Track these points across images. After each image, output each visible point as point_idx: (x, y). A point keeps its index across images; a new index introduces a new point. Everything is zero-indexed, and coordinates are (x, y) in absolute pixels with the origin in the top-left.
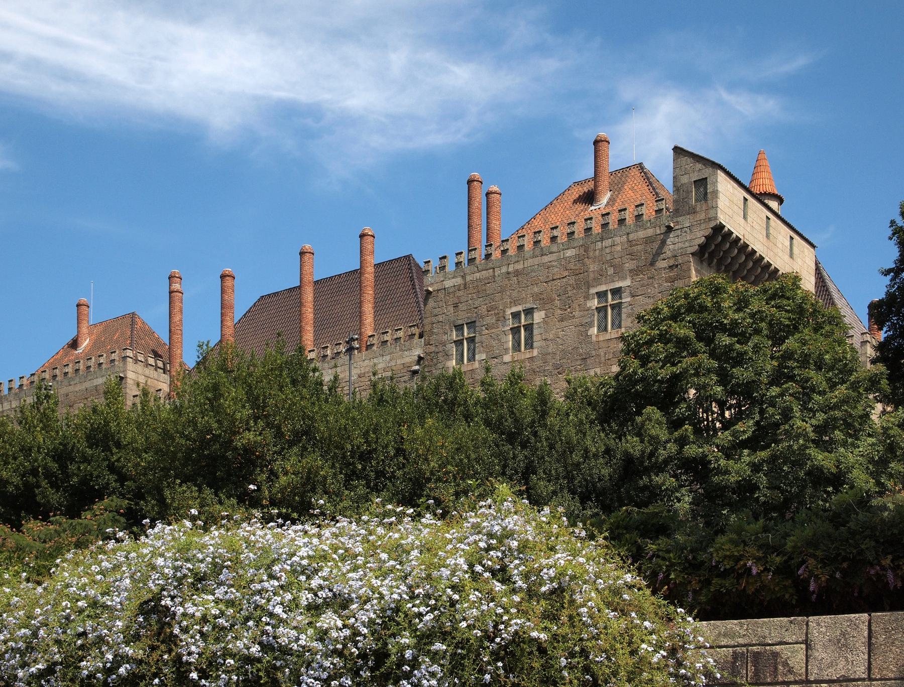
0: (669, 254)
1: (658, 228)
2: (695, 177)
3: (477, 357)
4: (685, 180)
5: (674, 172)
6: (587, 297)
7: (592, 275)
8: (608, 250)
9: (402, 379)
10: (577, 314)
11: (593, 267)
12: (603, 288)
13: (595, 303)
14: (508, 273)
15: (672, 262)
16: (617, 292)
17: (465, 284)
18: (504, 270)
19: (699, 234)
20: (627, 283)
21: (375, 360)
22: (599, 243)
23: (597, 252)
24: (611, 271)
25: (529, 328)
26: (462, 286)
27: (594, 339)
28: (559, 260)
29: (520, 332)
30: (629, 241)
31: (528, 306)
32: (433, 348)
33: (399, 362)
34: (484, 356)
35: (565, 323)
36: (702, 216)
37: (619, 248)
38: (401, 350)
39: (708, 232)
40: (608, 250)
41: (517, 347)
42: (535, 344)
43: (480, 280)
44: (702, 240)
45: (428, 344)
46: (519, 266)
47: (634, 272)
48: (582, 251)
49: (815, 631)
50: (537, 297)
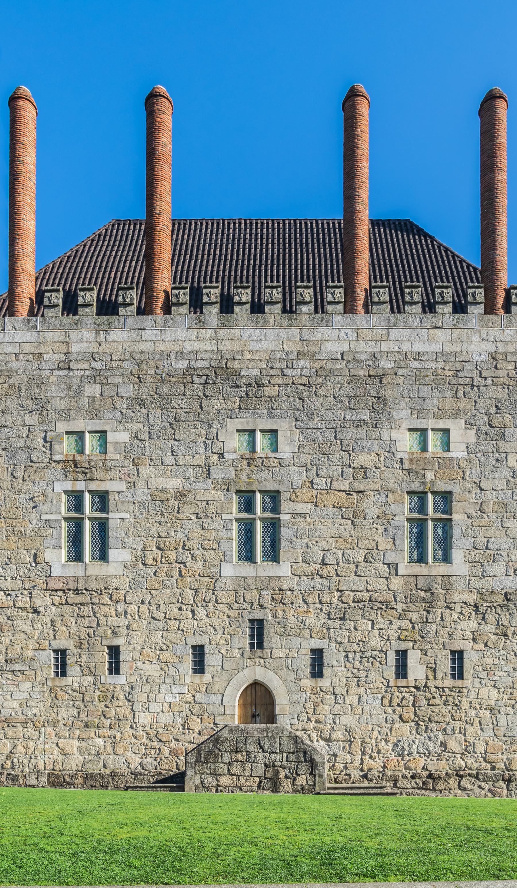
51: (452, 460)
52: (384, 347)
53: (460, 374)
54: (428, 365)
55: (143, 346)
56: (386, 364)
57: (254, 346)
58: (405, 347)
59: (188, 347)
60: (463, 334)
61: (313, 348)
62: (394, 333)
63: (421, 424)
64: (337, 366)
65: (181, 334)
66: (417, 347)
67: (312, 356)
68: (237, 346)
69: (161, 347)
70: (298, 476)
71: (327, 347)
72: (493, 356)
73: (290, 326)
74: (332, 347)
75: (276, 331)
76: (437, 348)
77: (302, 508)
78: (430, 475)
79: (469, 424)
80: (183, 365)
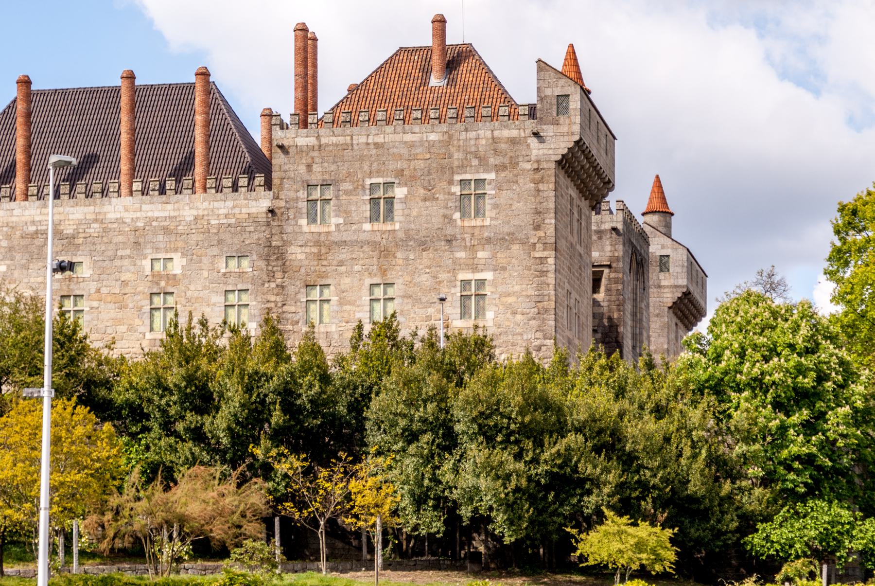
0: (533, 158)
1: (522, 130)
2: (558, 91)
3: (334, 220)
4: (548, 92)
5: (538, 83)
6: (451, 182)
7: (456, 163)
8: (473, 142)
9: (248, 229)
10: (441, 196)
11: (457, 155)
12: (467, 176)
13: (456, 189)
14: (368, 144)
15: (535, 166)
16: (479, 182)
17: (320, 146)
18: (363, 140)
19: (563, 145)
20: (492, 176)
21: (216, 204)
22: (464, 133)
23: (461, 142)
24: (475, 162)
25: (390, 201)
26: (316, 148)
27: (459, 222)
28: (421, 141)
29: (379, 204)
30: (493, 138)
31: (389, 180)
32: (282, 204)
33: (244, 210)
34: (341, 221)
35: (428, 203)
36: (565, 129)
37: (483, 142)
38: (247, 199)
39: (571, 145)
40: (473, 142)
41: (374, 217)
42: (396, 218)
43: (337, 145)
44: (565, 151)
45: (276, 197)
46: (380, 139)
47: (499, 168)
48: (446, 137)
49: (845, 513)
50: (400, 173)
51: (175, 275)
52: (139, 214)
53: (179, 228)
54: (162, 224)
55: (14, 219)
56: (140, 224)
57: (71, 217)
58: (150, 214)
59: (37, 218)
60: (181, 205)
61: (101, 217)
62: (144, 207)
63: (158, 256)
64: (115, 225)
65: (33, 212)
66: (156, 214)
67: (102, 223)
68: (62, 218)
69: (23, 219)
70: (93, 286)
71: (109, 216)
72: (196, 218)
73: (90, 205)
74: (111, 216)
75: (82, 208)
76: (166, 214)
77: (95, 304)
78: (163, 284)
79: (183, 255)
80: (33, 228)
